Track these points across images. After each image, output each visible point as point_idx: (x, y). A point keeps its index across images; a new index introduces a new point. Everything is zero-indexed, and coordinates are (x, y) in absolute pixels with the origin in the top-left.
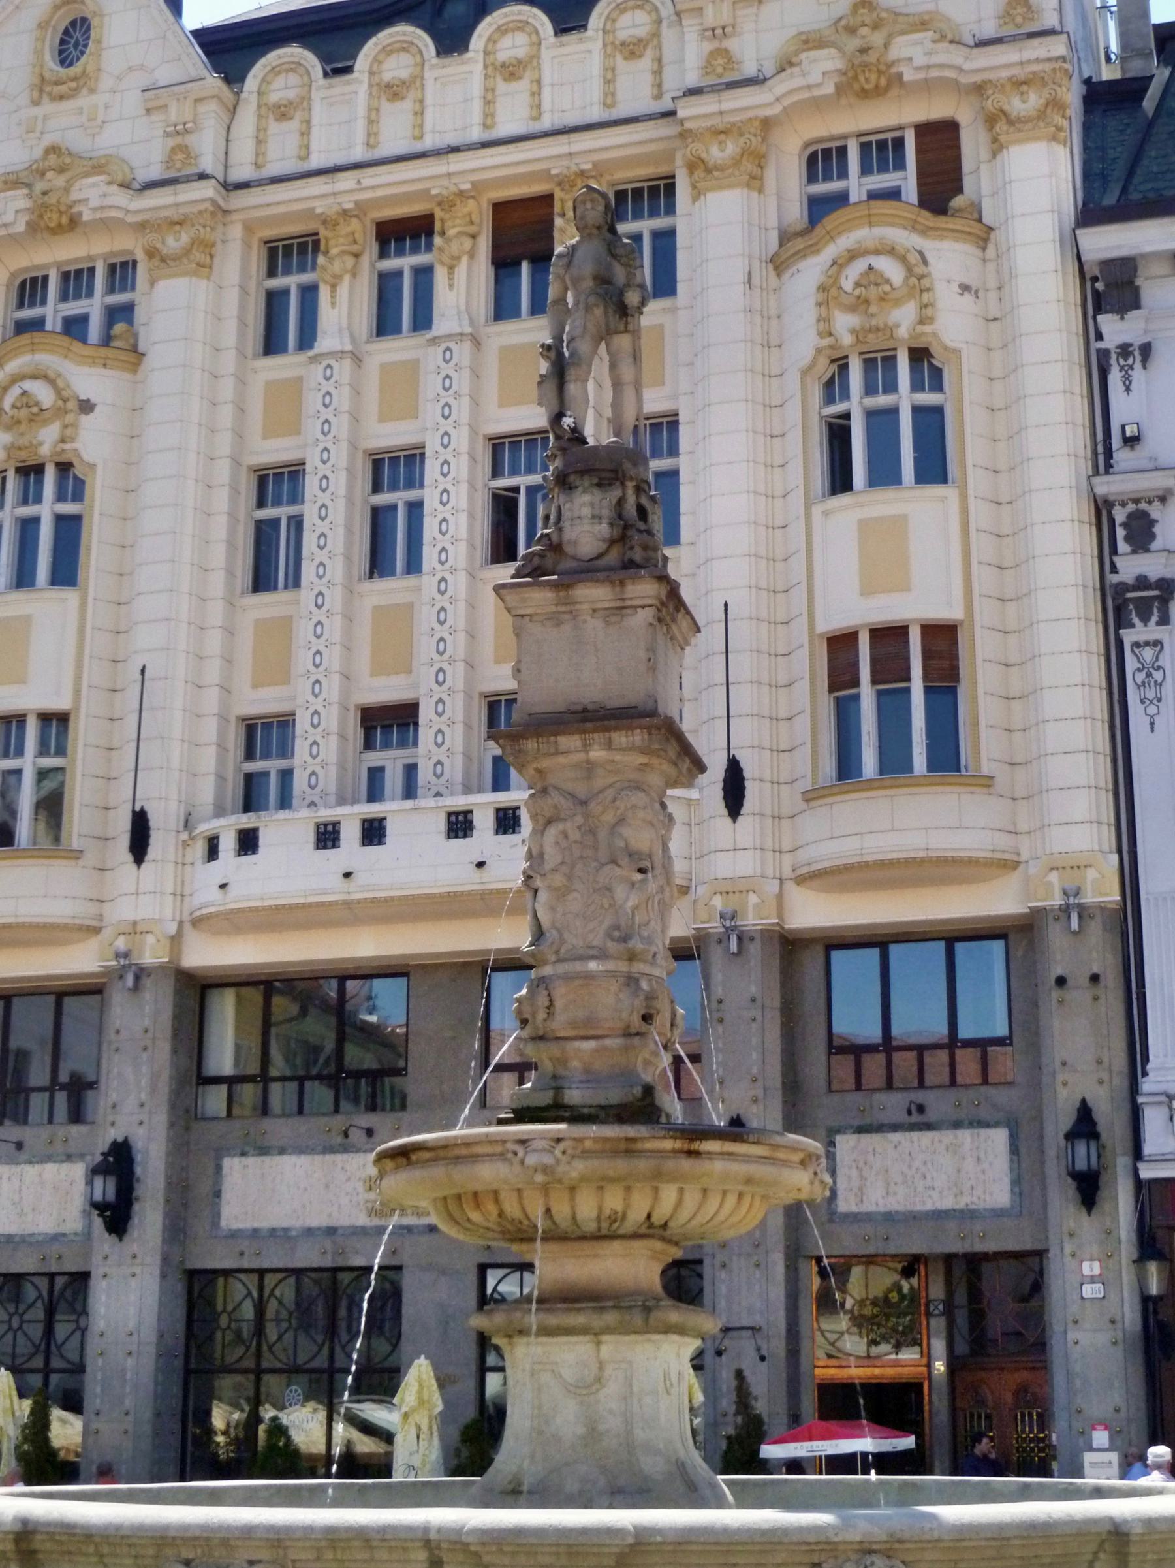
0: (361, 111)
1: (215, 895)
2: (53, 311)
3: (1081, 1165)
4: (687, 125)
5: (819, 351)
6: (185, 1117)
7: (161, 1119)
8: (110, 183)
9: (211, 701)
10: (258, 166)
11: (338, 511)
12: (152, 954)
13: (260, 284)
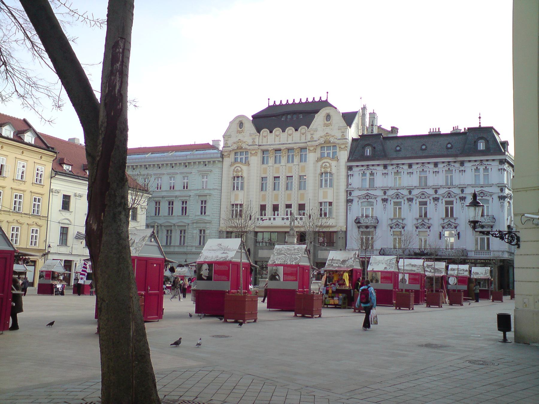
6: (255, 246)
7: (253, 246)
11: (271, 183)
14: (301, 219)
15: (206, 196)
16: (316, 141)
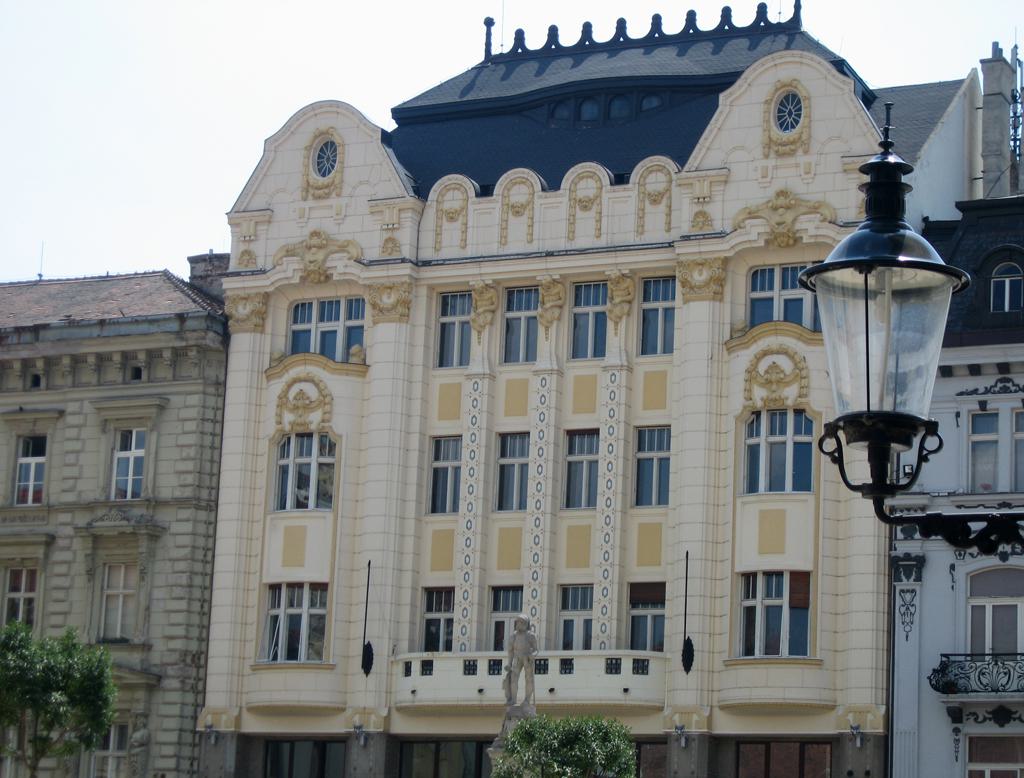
0: (497, 220)
1: (409, 696)
4: (682, 258)
5: (745, 407)
8: (349, 259)
9: (407, 580)
10: (437, 250)
11: (480, 473)
12: (374, 726)
13: (436, 320)
14: (640, 667)
16: (721, 235)
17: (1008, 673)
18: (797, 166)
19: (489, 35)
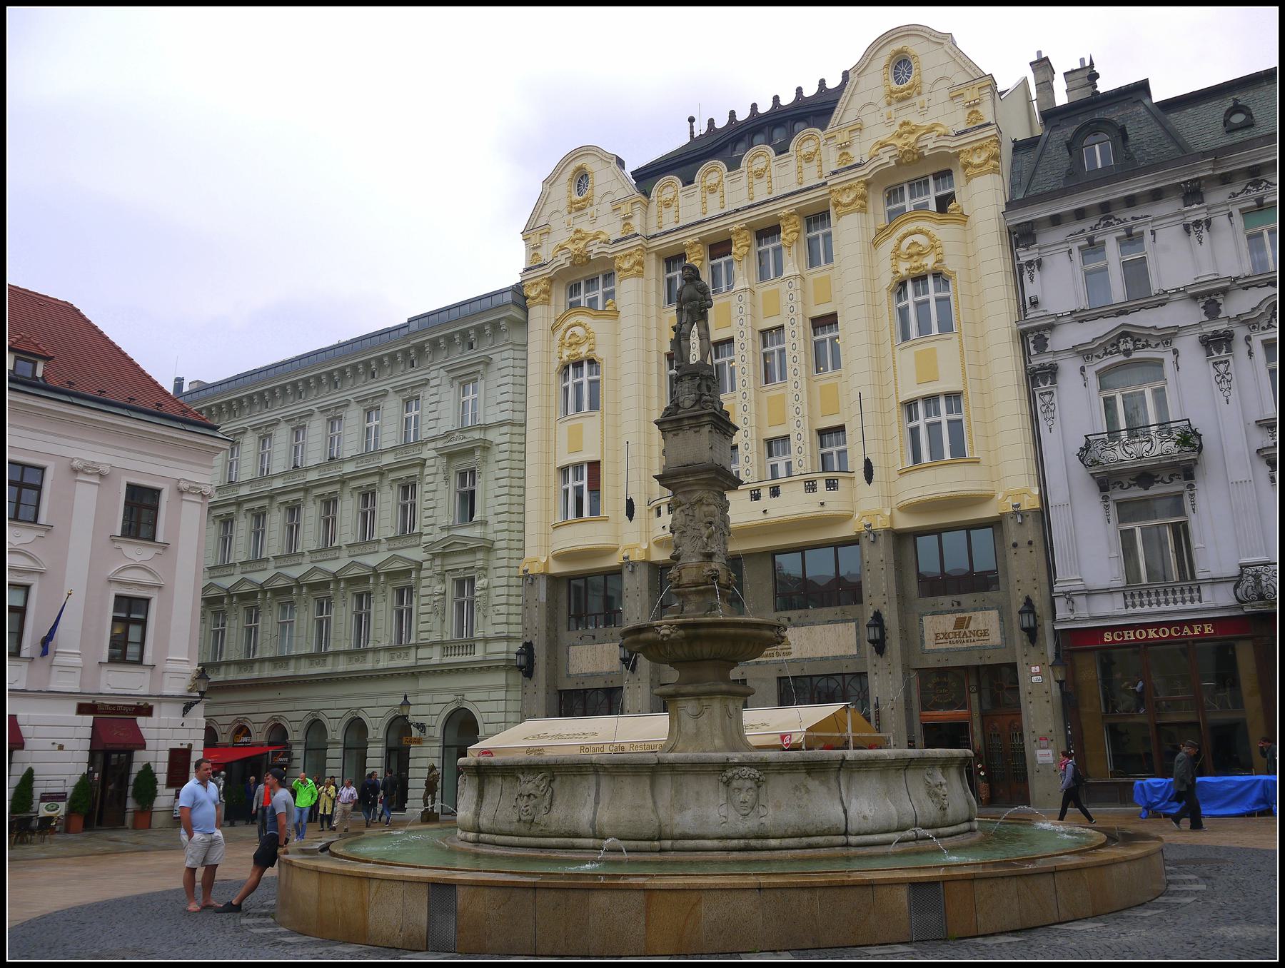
2: (583, 297)
3: (1026, 625)
14: (831, 484)
15: (471, 451)
17: (1150, 441)
18: (913, 105)
19: (692, 127)
